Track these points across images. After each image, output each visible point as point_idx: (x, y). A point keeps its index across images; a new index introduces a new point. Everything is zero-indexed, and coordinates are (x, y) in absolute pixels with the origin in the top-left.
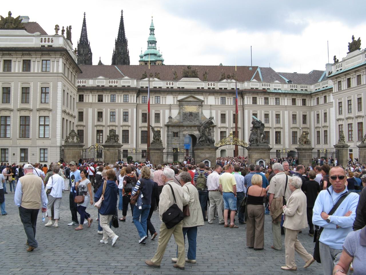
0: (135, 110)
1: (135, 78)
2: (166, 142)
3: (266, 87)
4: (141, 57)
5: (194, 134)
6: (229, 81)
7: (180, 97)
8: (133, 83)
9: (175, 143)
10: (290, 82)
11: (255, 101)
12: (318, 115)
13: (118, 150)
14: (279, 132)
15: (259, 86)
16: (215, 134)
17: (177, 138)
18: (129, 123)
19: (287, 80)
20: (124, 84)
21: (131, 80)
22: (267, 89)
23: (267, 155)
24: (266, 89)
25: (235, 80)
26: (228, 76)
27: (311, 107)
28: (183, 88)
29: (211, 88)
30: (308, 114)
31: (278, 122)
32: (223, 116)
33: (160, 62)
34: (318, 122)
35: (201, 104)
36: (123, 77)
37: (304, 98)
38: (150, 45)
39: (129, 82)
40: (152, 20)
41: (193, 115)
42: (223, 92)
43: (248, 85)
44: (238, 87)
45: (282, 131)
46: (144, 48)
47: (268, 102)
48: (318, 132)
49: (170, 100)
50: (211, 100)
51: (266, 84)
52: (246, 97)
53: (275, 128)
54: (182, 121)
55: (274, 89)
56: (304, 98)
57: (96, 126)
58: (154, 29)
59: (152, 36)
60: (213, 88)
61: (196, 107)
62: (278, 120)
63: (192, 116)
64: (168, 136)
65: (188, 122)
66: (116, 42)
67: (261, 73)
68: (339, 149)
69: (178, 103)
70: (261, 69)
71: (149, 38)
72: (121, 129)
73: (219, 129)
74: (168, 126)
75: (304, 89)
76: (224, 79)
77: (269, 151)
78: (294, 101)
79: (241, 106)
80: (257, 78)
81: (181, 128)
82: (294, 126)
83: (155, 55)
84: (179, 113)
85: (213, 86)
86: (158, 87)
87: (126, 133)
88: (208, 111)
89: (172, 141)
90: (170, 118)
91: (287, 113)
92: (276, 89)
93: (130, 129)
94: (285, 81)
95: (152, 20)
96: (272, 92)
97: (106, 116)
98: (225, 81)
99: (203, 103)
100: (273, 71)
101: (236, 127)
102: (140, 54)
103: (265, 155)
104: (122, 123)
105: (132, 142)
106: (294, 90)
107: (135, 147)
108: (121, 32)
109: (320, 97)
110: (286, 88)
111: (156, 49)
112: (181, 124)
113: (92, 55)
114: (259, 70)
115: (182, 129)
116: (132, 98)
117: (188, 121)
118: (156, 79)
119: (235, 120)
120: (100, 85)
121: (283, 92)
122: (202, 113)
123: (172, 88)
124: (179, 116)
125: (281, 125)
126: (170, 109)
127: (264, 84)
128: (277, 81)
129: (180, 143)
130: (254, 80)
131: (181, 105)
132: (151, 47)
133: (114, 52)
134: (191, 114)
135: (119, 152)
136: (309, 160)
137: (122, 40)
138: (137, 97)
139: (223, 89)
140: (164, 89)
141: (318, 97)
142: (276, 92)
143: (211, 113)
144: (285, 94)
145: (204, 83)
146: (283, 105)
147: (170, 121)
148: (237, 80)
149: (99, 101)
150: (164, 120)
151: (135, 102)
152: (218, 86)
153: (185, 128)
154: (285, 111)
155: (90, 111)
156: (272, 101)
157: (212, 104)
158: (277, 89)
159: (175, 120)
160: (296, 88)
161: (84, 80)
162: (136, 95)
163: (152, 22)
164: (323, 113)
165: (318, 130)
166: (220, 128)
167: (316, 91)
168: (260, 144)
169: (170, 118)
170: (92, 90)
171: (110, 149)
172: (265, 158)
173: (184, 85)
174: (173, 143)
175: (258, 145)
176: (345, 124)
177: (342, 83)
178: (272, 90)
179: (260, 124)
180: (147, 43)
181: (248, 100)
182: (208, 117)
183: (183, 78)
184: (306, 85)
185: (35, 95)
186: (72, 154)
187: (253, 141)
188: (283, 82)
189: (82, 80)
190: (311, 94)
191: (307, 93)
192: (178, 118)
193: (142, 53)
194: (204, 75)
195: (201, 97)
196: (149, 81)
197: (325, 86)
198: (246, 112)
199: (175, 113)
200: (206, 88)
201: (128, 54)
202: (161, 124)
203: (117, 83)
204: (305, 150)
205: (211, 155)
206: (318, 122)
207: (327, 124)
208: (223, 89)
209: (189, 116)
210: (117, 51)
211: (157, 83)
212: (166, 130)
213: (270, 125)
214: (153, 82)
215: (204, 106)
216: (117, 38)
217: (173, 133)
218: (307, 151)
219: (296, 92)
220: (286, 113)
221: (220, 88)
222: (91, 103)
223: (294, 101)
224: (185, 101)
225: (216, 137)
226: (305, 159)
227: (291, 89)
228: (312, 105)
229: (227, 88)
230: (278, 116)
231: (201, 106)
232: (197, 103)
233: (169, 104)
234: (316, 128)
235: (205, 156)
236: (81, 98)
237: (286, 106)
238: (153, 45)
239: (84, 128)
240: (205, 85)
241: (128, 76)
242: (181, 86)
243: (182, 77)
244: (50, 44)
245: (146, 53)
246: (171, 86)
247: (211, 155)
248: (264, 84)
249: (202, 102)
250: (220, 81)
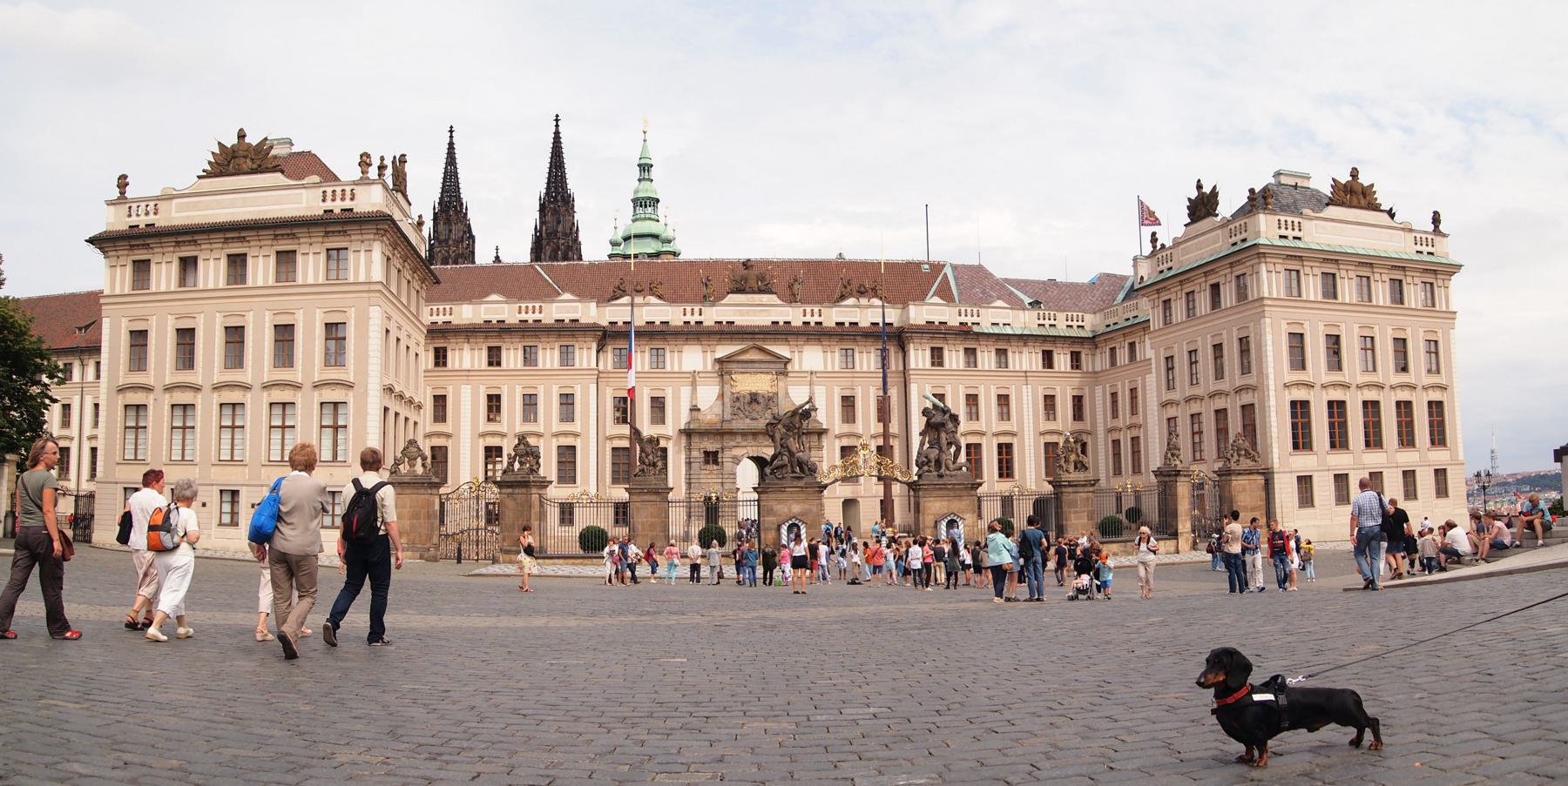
1: (592, 297)
2: (683, 480)
3: (969, 320)
4: (614, 244)
5: (764, 456)
6: (864, 301)
7: (724, 350)
8: (591, 313)
9: (710, 481)
10: (1036, 304)
11: (937, 357)
12: (1114, 395)
13: (539, 494)
14: (1009, 446)
15: (951, 316)
16: (825, 456)
17: (715, 467)
18: (576, 427)
19: (1027, 300)
22: (973, 324)
23: (968, 502)
24: (970, 324)
25: (881, 299)
26: (860, 288)
27: (1096, 373)
29: (812, 324)
30: (1086, 393)
32: (848, 403)
33: (671, 259)
34: (1115, 415)
35: (781, 367)
36: (559, 294)
37: (1076, 349)
38: (640, 210)
40: (645, 141)
41: (761, 400)
42: (846, 335)
44: (887, 321)
45: (1015, 441)
46: (625, 221)
47: (975, 362)
48: (1116, 443)
49: (693, 358)
50: (811, 358)
51: (969, 309)
53: (997, 435)
54: (727, 416)
55: (992, 324)
56: (1076, 349)
57: (483, 435)
58: (652, 166)
59: (646, 184)
61: (769, 377)
62: (1005, 410)
63: (758, 403)
64: (689, 464)
65: (748, 421)
66: (540, 205)
67: (956, 278)
68: (1167, 479)
69: (717, 367)
70: (955, 268)
71: (636, 192)
72: (554, 444)
73: (837, 441)
74: (688, 433)
75: (1075, 324)
76: (851, 295)
77: (973, 492)
79: (900, 372)
80: (945, 294)
81: (726, 437)
82: (1051, 426)
83: (655, 237)
84: (722, 396)
85: (816, 315)
86: (658, 323)
87: (567, 456)
89: (702, 476)
90: (694, 409)
91: (1030, 390)
92: (998, 324)
93: (578, 443)
94: (1022, 301)
95: (645, 141)
96: (986, 331)
97: (512, 406)
98: (851, 301)
99: (789, 367)
100: (988, 275)
101: (886, 435)
102: (610, 235)
103: (964, 503)
104: (557, 426)
105: (586, 482)
106: (1047, 326)
108: (556, 176)
109: (1118, 346)
110: (1025, 321)
111: (658, 221)
112: (726, 426)
113: (474, 242)
114: (948, 271)
115: (729, 442)
116: (585, 355)
118: (653, 299)
119: (883, 414)
120: (494, 318)
121: (1019, 332)
122: (787, 393)
124: (719, 402)
125: (1011, 426)
126: (694, 384)
127: (963, 309)
128: (1000, 303)
129: (724, 481)
130: (936, 300)
131: (726, 373)
132: (643, 216)
133: (536, 234)
134: (754, 398)
135: (540, 501)
136: (1086, 514)
137: (559, 198)
138: (598, 352)
139: (847, 325)
140: (676, 327)
141: (1113, 346)
142: (997, 332)
144: (1024, 339)
145: (790, 309)
146: (1018, 368)
148: (888, 300)
149: (490, 364)
150: (678, 416)
151: (593, 365)
152: (831, 316)
153: (739, 439)
154: (1025, 386)
155: (466, 391)
156: (987, 358)
157: (815, 369)
158: (1001, 325)
159: (709, 417)
160: (1052, 322)
161: (448, 307)
162: (594, 346)
163: (644, 148)
164: (1127, 389)
165: (1115, 436)
166: (840, 437)
167: (1109, 329)
168: (948, 472)
169: (694, 409)
170: (469, 332)
171: (517, 491)
172: (963, 512)
173: (735, 315)
174: (702, 481)
175: (941, 476)
176: (1182, 414)
177: (1173, 304)
178: (986, 327)
179: (947, 416)
180: (632, 204)
183: (730, 295)
184: (1080, 314)
185: (310, 343)
186: (410, 507)
187: (927, 464)
188: (1015, 304)
189: (441, 308)
190: (1094, 337)
191: (1082, 334)
192: (718, 410)
193: (616, 233)
194: (791, 287)
195: (782, 350)
196: (632, 305)
197: (1130, 315)
198: (914, 389)
199: (708, 396)
200: (797, 322)
201: (577, 236)
202: (670, 428)
203: (540, 312)
204: (1076, 486)
205: (806, 506)
206: (1115, 415)
207: (1140, 419)
208: (847, 325)
209: (750, 403)
210: (544, 228)
211: (652, 311)
212: (683, 445)
213: (981, 426)
214: (645, 308)
215: (790, 375)
216: (544, 191)
217: (705, 452)
218: (1081, 489)
219: (1052, 332)
220: (1027, 391)
221: (837, 323)
222: (469, 371)
224: (738, 362)
225: (827, 458)
226: (1075, 512)
227: (1039, 325)
228: (1098, 368)
229: (857, 324)
230: (1003, 400)
232: (772, 366)
233: (692, 370)
234: (1110, 431)
235: (790, 511)
236: (440, 357)
237: (1026, 372)
238: (650, 210)
239: (450, 441)
240: (794, 315)
241: (573, 293)
242: (724, 319)
243: (728, 293)
245: (627, 234)
246: (697, 318)
247: (806, 506)
248: (963, 309)
249: (786, 364)
250: (838, 302)
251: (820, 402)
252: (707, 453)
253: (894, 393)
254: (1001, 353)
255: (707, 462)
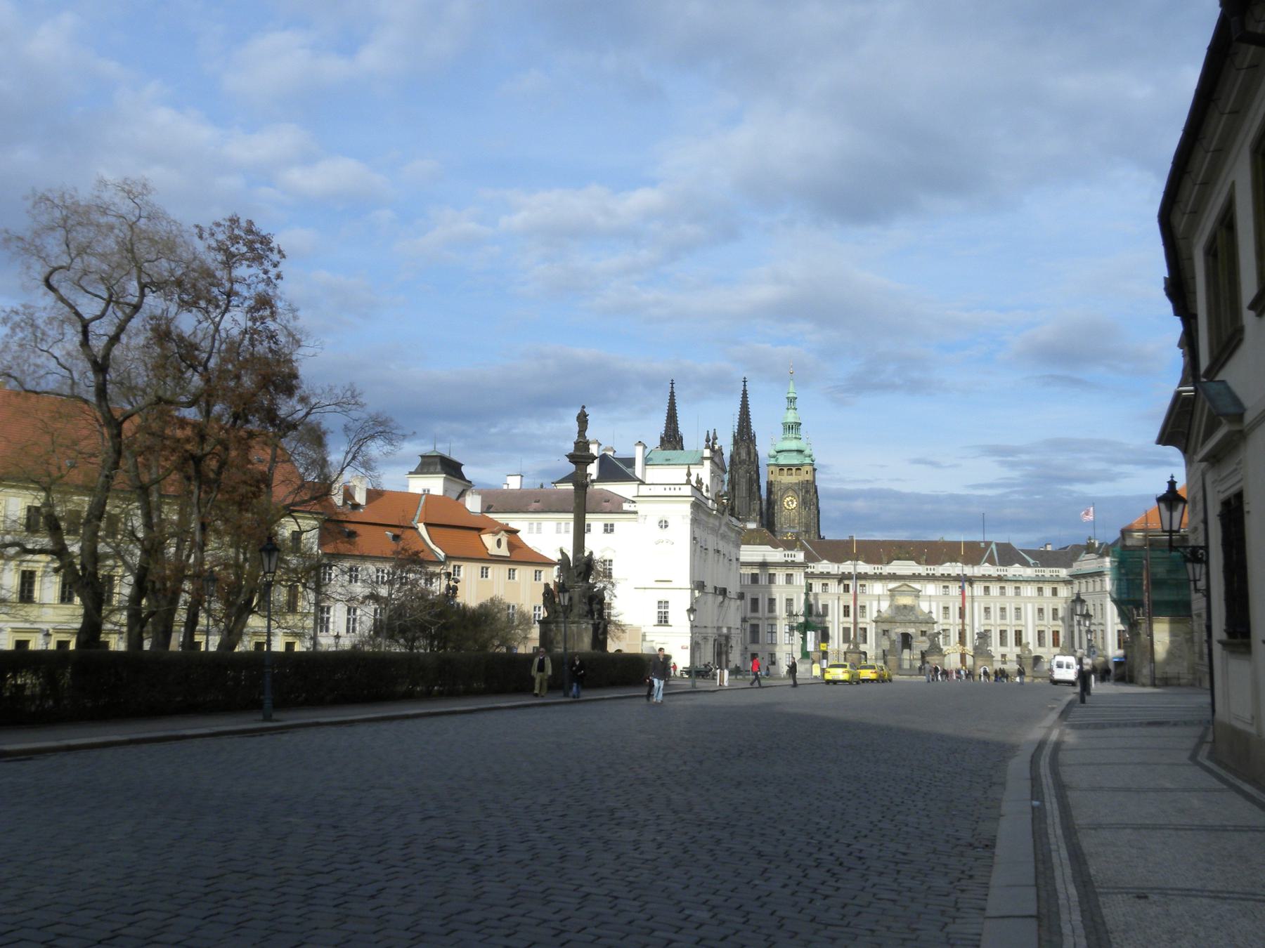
0: (836, 601)
3: (1002, 573)
6: (954, 564)
11: (987, 589)
20: (822, 570)
21: (830, 566)
28: (894, 574)
31: (1018, 617)
32: (946, 609)
35: (917, 594)
39: (829, 568)
43: (979, 571)
49: (878, 588)
50: (931, 589)
52: (975, 586)
53: (1014, 626)
56: (1055, 586)
60: (933, 574)
64: (877, 634)
65: (902, 617)
67: (997, 551)
69: (889, 593)
70: (997, 545)
74: (876, 622)
78: (1040, 590)
80: (991, 561)
83: (800, 452)
84: (890, 606)
88: (928, 603)
98: (948, 564)
101: (963, 624)
107: (836, 647)
117: (902, 615)
123: (881, 573)
126: (879, 600)
130: (987, 564)
134: (905, 607)
143: (930, 605)
144: (1028, 581)
147: (878, 616)
148: (966, 562)
150: (872, 613)
153: (898, 624)
169: (879, 611)
181: (978, 589)
182: (926, 611)
188: (1025, 564)
192: (889, 612)
195: (917, 585)
198: (976, 604)
199: (885, 606)
200: (924, 574)
202: (868, 620)
211: (863, 567)
223: (1040, 590)
230: (1018, 609)
231: (917, 596)
241: (829, 560)
242: (892, 572)
244: (793, 559)
246: (880, 571)
251: (934, 610)
252: (884, 631)
253: (968, 605)
254: (1017, 588)
255: (884, 634)
